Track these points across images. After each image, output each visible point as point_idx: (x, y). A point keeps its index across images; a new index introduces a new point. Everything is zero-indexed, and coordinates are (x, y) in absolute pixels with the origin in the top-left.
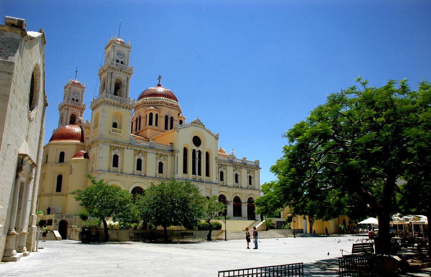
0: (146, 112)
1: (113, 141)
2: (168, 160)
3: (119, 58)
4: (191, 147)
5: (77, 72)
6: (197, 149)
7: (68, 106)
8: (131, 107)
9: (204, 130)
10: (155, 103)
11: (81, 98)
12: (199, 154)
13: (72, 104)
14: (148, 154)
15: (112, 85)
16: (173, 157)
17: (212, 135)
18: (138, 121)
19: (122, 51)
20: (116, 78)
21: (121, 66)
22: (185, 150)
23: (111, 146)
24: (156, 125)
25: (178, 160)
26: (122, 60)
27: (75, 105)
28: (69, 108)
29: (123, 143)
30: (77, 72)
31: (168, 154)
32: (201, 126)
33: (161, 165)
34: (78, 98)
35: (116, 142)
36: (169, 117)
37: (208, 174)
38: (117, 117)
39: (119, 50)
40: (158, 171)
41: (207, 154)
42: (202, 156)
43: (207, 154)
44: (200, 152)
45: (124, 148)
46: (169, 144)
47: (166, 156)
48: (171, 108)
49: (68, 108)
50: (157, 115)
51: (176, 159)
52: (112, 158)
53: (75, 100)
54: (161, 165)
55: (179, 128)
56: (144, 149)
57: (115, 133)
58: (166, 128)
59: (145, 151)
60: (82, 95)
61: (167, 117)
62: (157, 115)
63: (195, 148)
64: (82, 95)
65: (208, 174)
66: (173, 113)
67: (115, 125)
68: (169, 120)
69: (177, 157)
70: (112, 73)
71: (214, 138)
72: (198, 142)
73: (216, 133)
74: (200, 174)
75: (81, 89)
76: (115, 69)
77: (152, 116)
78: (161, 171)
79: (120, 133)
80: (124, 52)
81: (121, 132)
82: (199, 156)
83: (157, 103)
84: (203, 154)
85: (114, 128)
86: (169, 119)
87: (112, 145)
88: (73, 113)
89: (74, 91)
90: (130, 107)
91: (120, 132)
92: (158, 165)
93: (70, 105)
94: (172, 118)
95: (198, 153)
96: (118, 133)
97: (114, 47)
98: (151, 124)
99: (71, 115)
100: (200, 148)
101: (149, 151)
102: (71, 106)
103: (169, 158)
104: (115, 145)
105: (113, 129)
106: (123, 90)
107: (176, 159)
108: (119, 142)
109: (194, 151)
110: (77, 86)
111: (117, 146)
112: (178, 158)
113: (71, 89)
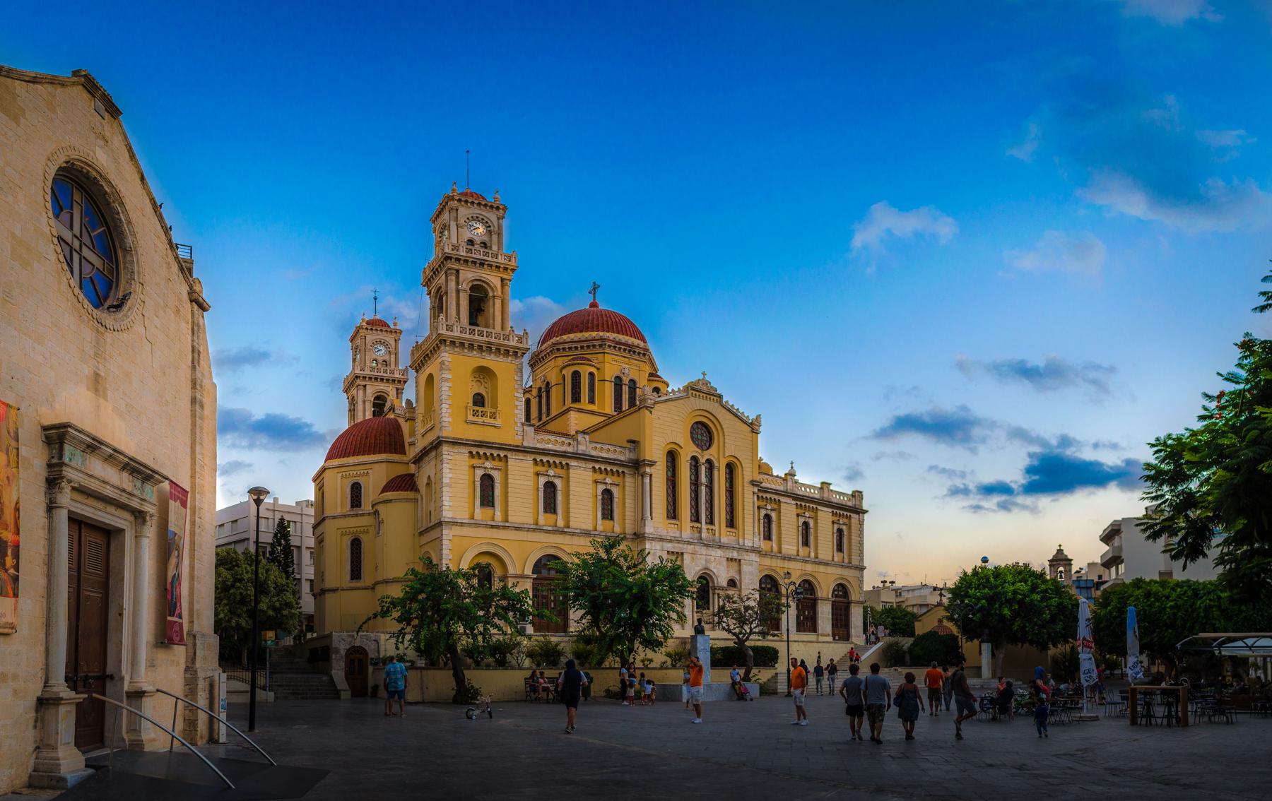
0: (561, 371)
1: (476, 441)
2: (627, 484)
4: (688, 450)
10: (585, 348)
14: (571, 471)
16: (640, 478)
22: (672, 456)
25: (653, 484)
36: (626, 380)
41: (730, 468)
44: (709, 461)
51: (647, 480)
57: (480, 419)
61: (618, 382)
69: (651, 475)
79: (494, 418)
86: (624, 387)
91: (493, 416)
101: (573, 463)
103: (629, 481)
104: (481, 451)
105: (473, 411)
109: (694, 458)
112: (653, 479)
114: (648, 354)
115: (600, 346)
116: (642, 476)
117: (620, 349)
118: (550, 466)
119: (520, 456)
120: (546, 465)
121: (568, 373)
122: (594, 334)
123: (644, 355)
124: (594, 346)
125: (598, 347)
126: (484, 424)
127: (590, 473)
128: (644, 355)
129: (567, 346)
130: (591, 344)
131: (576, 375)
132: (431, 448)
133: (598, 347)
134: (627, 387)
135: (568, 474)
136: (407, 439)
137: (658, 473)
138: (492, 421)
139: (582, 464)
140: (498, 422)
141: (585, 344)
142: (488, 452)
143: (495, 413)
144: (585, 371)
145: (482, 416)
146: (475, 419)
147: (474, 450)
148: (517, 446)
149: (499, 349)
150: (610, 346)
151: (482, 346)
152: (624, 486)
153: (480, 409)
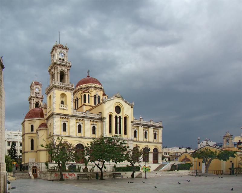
4: (115, 114)
6: (118, 115)
22: (110, 116)
24: (89, 102)
25: (106, 124)
31: (98, 121)
33: (94, 128)
35: (64, 115)
36: (97, 96)
41: (126, 118)
44: (120, 117)
51: (104, 123)
54: (94, 128)
57: (62, 108)
68: (97, 98)
69: (105, 122)
91: (66, 107)
92: (92, 128)
94: (99, 96)
103: (99, 123)
104: (63, 117)
109: (116, 117)
116: (103, 122)
119: (72, 118)
126: (64, 109)
127: (90, 122)
137: (107, 121)
139: (87, 119)
144: (87, 94)
153: (63, 105)
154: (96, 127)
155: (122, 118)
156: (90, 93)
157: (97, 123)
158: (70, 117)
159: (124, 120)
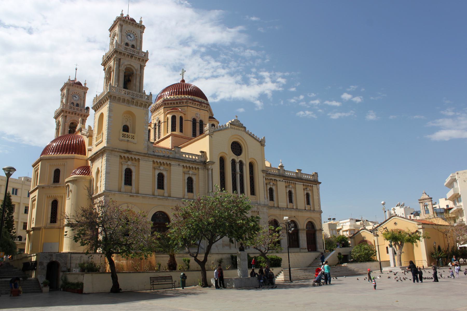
0: (166, 116)
1: (124, 150)
2: (200, 174)
3: (128, 41)
4: (230, 156)
5: (76, 69)
6: (238, 159)
7: (66, 112)
8: (148, 105)
9: (245, 133)
10: (178, 103)
11: (82, 102)
12: (240, 166)
13: (71, 110)
14: (172, 167)
15: (120, 76)
16: (207, 171)
17: (255, 139)
18: (157, 127)
19: (132, 32)
20: (125, 67)
21: (132, 51)
22: (222, 160)
23: (121, 156)
24: (181, 131)
25: (213, 174)
26: (134, 43)
27: (75, 111)
28: (68, 114)
29: (139, 154)
30: (76, 69)
31: (199, 167)
32: (241, 129)
33: (190, 181)
34: (79, 102)
35: (128, 151)
36: (198, 120)
37: (253, 192)
38: (128, 118)
39: (129, 31)
40: (186, 190)
41: (251, 166)
42: (244, 167)
43: (251, 166)
44: (241, 163)
45: (139, 159)
46: (200, 154)
47: (197, 170)
48: (200, 109)
49: (66, 114)
50: (181, 118)
51: (210, 172)
52: (124, 173)
53: (75, 104)
54: (190, 181)
55: (212, 131)
56: (167, 161)
57: (126, 139)
58: (194, 135)
59: (168, 163)
60: (84, 98)
61: (194, 121)
62: (181, 118)
63: (235, 157)
64: (84, 98)
65: (253, 192)
66: (202, 115)
67: (126, 129)
68: (198, 125)
69: (212, 169)
70: (120, 59)
71: (259, 144)
72: (238, 149)
73: (261, 138)
74: (242, 191)
75: (82, 90)
76: (124, 54)
77: (176, 120)
78: (190, 189)
79: (133, 139)
80: (135, 33)
81: (135, 137)
82: (240, 168)
83: (181, 103)
84: (246, 165)
85: (125, 133)
86: (197, 124)
87: (123, 155)
88: (73, 121)
89: (74, 93)
90: (146, 104)
91: (133, 138)
92: (186, 181)
93: (68, 111)
95: (239, 164)
96: (130, 139)
97: (122, 26)
98: (173, 129)
99: (70, 123)
100: (241, 158)
101: (173, 163)
102: (69, 112)
103: (201, 172)
104: (126, 155)
105: (123, 134)
106: (135, 82)
107: (210, 172)
108: (132, 152)
109: (233, 162)
110: (78, 87)
111: (130, 156)
112: (213, 171)
113: (70, 90)
114: (208, 106)
115: (186, 102)
116: (208, 170)
117: (195, 104)
118: (161, 164)
120: (159, 164)
121: (170, 116)
122: (183, 96)
123: (207, 107)
124: (183, 102)
125: (184, 103)
128: (207, 107)
129: (169, 102)
130: (181, 101)
131: (174, 118)
132: (100, 153)
133: (184, 103)
134: (199, 124)
135: (170, 169)
136: (87, 147)
137: (216, 168)
138: (132, 140)
140: (135, 141)
141: (178, 101)
142: (130, 156)
143: (134, 136)
145: (127, 137)
146: (124, 138)
147: (123, 155)
148: (145, 154)
149: (138, 102)
150: (190, 103)
151: (129, 100)
152: (199, 175)
153: (126, 133)
154: (194, 178)
155: (244, 162)
156: (185, 114)
157: (196, 172)
158: (140, 157)
159: (250, 168)
